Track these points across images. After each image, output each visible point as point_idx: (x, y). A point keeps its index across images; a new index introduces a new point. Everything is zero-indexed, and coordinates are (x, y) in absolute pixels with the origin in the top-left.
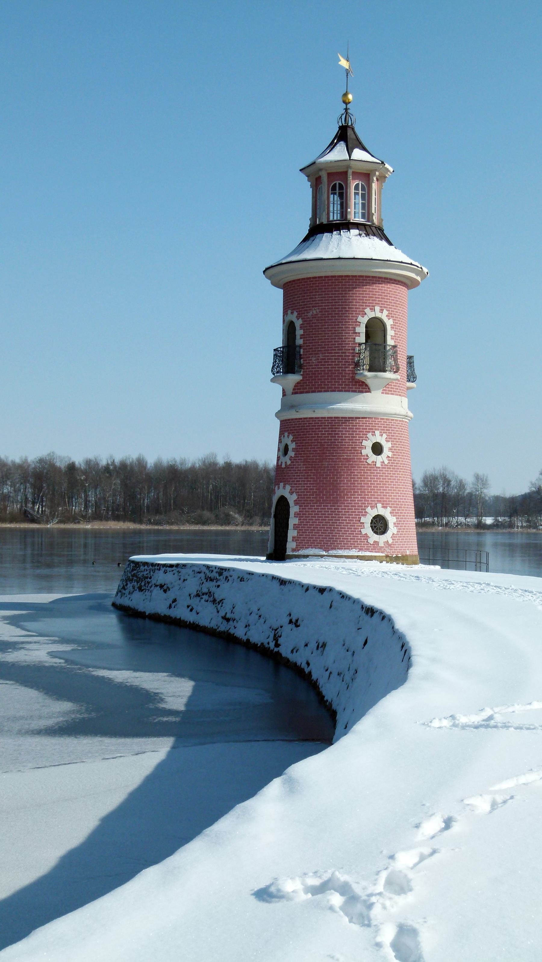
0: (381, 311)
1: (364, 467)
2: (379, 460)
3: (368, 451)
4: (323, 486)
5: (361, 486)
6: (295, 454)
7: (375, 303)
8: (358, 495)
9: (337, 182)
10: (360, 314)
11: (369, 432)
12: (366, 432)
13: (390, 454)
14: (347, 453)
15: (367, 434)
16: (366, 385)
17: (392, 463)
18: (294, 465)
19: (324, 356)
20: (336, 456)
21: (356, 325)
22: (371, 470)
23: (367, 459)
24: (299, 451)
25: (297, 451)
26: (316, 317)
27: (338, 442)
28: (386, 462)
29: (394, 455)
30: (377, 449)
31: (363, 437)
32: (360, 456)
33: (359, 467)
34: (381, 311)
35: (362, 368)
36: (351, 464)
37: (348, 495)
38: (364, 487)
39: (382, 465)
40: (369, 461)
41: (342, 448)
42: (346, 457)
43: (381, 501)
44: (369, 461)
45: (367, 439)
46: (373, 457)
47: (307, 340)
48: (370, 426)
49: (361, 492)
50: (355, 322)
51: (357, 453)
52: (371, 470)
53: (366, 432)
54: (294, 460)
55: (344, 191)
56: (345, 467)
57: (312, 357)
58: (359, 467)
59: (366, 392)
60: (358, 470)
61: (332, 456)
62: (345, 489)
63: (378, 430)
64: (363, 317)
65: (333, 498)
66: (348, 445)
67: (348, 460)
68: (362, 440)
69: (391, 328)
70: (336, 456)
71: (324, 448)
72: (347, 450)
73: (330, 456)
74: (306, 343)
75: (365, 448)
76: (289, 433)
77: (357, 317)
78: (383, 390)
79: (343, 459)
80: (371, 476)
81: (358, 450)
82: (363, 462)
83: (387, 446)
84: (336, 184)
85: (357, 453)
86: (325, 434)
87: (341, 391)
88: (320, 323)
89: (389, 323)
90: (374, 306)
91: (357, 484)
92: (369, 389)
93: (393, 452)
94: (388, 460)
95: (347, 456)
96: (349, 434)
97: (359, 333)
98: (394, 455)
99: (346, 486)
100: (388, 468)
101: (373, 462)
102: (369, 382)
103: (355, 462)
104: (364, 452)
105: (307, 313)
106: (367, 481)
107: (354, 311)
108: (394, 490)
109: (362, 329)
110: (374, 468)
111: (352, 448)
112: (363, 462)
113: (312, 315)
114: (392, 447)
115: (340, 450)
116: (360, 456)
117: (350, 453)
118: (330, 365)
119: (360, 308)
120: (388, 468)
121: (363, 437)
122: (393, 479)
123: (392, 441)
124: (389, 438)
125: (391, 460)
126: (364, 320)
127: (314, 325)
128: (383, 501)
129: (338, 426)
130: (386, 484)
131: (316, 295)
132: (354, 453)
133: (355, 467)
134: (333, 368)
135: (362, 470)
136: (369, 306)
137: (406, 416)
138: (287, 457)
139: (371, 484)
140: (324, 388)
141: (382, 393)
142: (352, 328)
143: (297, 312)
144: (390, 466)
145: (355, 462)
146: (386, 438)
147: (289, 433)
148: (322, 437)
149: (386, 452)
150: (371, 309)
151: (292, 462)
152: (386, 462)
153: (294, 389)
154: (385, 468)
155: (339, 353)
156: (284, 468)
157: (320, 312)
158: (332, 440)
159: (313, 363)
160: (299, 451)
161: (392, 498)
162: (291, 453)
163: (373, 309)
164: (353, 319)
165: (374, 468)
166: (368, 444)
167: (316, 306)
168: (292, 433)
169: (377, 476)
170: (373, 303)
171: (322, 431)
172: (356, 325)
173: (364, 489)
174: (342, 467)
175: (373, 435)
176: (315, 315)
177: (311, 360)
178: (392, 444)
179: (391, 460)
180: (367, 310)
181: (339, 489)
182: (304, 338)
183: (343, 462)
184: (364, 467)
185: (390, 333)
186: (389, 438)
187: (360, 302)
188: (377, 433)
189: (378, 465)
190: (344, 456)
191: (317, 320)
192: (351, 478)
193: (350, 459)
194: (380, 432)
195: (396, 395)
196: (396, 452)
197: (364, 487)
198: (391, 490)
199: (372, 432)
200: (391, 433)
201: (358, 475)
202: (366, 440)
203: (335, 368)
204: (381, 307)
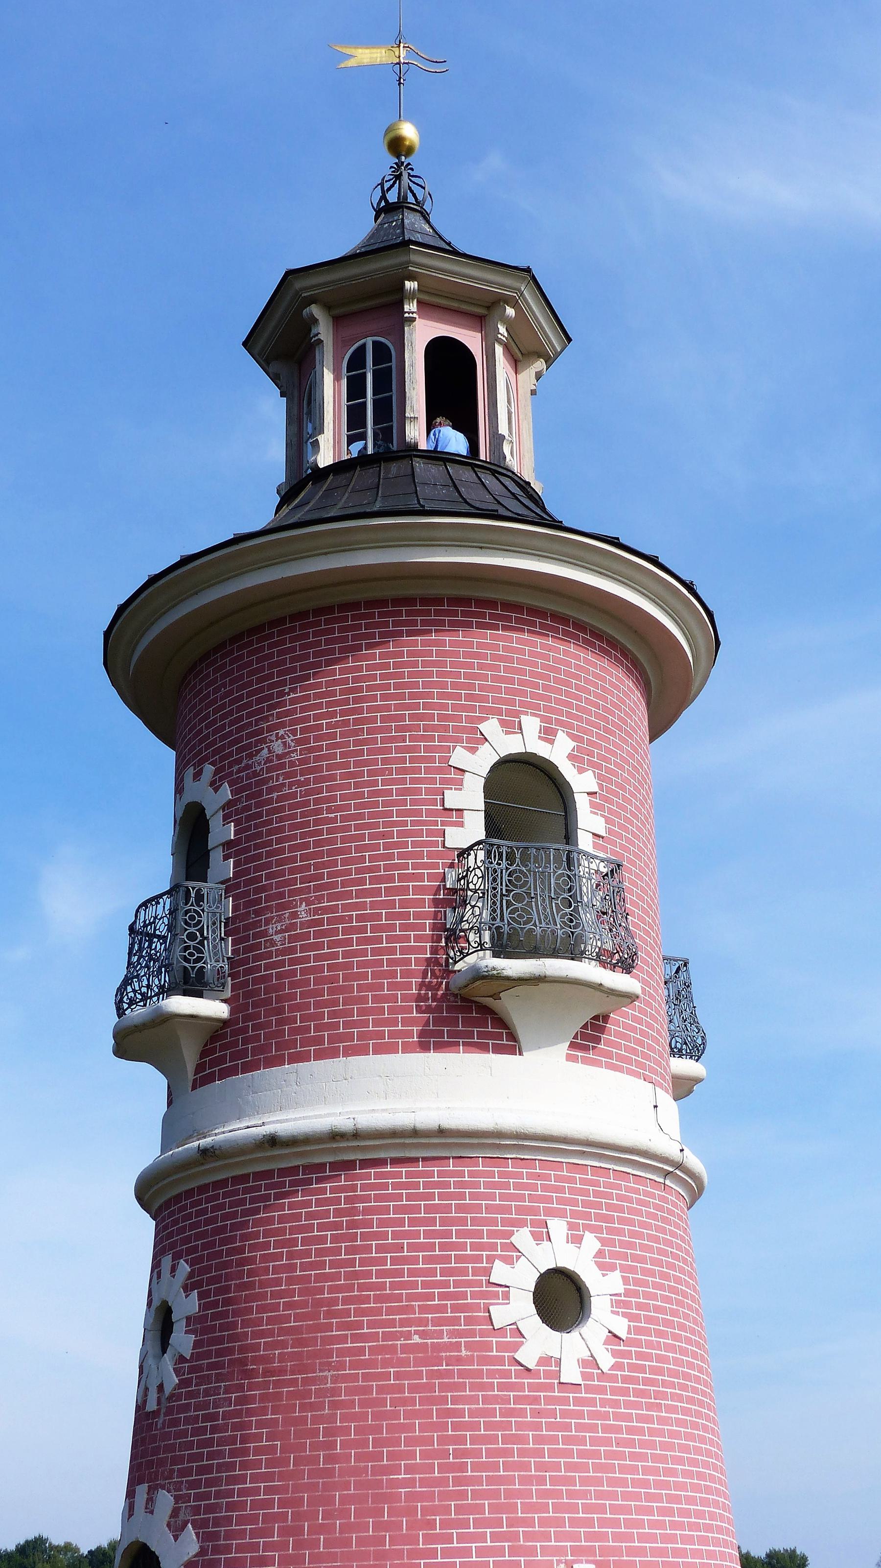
0: (548, 735)
1: (502, 1387)
2: (569, 1351)
3: (519, 1309)
4: (313, 1487)
5: (490, 1480)
6: (197, 1344)
7: (522, 704)
8: (478, 1523)
9: (369, 342)
10: (459, 740)
11: (521, 1224)
12: (505, 1222)
13: (621, 1327)
14: (425, 1322)
15: (512, 1233)
16: (502, 1023)
17: (633, 1368)
18: (190, 1395)
19: (316, 911)
20: (374, 1337)
21: (443, 781)
22: (536, 1400)
23: (516, 1347)
24: (213, 1329)
25: (205, 1331)
26: (282, 766)
27: (380, 1274)
28: (606, 1361)
29: (638, 1331)
30: (561, 1299)
31: (493, 1247)
32: (483, 1333)
33: (482, 1387)
34: (548, 735)
35: (472, 937)
36: (440, 1374)
37: (431, 1525)
38: (510, 1480)
39: (585, 1376)
40: (528, 1356)
41: (399, 1298)
42: (416, 1339)
43: (590, 1551)
44: (528, 1356)
45: (511, 1254)
46: (539, 1341)
47: (248, 860)
48: (521, 1198)
49: (493, 1508)
50: (439, 770)
51: (469, 1321)
52: (536, 1400)
53: (505, 1222)
54: (192, 1370)
55: (394, 364)
56: (413, 1389)
57: (268, 922)
58: (482, 1387)
59: (499, 1050)
60: (474, 1400)
61: (356, 1338)
62: (422, 1497)
63: (561, 1214)
64: (473, 750)
65: (361, 1542)
66: (425, 1285)
67: (430, 1355)
68: (491, 1260)
69: (593, 805)
70: (374, 1337)
71: (320, 1303)
72: (424, 1309)
73: (344, 1340)
74: (247, 871)
75: (506, 1296)
76: (177, 1257)
77: (448, 750)
78: (573, 1046)
79: (405, 1348)
80: (537, 1427)
81: (477, 1307)
82: (500, 1361)
83: (602, 1286)
84: (363, 346)
85: (469, 1321)
86: (322, 1240)
87: (391, 1049)
88: (300, 784)
89: (581, 783)
90: (517, 714)
91: (476, 1467)
92: (512, 1037)
93: (631, 1317)
94: (615, 1354)
95: (423, 1335)
96: (427, 1235)
97: (460, 811)
98: (638, 1331)
99: (423, 1482)
100: (614, 1391)
101: (545, 1360)
102: (510, 1005)
103: (459, 1360)
104: (501, 1315)
105: (250, 756)
106: (522, 1453)
107: (434, 728)
108: (650, 1497)
109: (470, 797)
110: (550, 1387)
111: (442, 1296)
112: (500, 1361)
113: (269, 760)
114: (627, 1293)
115: (390, 1311)
116: (483, 1333)
117: (437, 1322)
118: (339, 944)
119: (459, 719)
120: (614, 1391)
121: (493, 1247)
122: (643, 1444)
123: (623, 1269)
124: (613, 1255)
125: (628, 1355)
126: (478, 764)
127: (275, 795)
128: (604, 1551)
129: (378, 1198)
130: (611, 1468)
131: (283, 683)
132: (455, 1321)
133: (461, 1387)
134: (355, 953)
135: (496, 1399)
136: (499, 712)
137: (679, 1166)
138: (168, 1360)
139: (540, 1467)
140: (319, 1040)
141: (569, 1058)
142: (429, 791)
143: (212, 764)
144: (625, 1379)
145: (459, 1360)
146: (600, 1254)
147: (177, 1257)
148: (308, 1254)
149: (603, 1317)
150: (503, 723)
151: (183, 1383)
152: (606, 1361)
153: (199, 1068)
154: (602, 1390)
155: (377, 892)
156: (159, 1411)
157: (299, 742)
158: (352, 1263)
159: (273, 943)
160: (213, 1329)
161: (643, 1538)
162: (183, 1341)
163: (512, 726)
164: (432, 760)
165: (550, 1387)
166: (520, 1278)
167: (282, 725)
168: (189, 1251)
169: (567, 1427)
170: (512, 703)
171: (310, 1228)
172: (443, 781)
173: (509, 1494)
174: (400, 1389)
175: (537, 1237)
176: (279, 757)
177: (264, 934)
178: (626, 1281)
179: (628, 1355)
180: (490, 727)
181: (393, 1498)
182: (237, 854)
183: (405, 1363)
184: (502, 1387)
185: (589, 822)
186: (613, 1255)
187: (458, 697)
188: (558, 1227)
189: (571, 1373)
190: (408, 1336)
191: (287, 776)
192: (443, 1440)
193: (437, 1347)
194: (572, 1226)
195: (630, 1072)
196: (649, 1320)
197: (510, 1480)
198: (636, 1497)
199: (534, 1224)
200: (619, 1232)
201: (475, 1426)
202: (509, 1261)
203: (364, 953)
204: (543, 719)
